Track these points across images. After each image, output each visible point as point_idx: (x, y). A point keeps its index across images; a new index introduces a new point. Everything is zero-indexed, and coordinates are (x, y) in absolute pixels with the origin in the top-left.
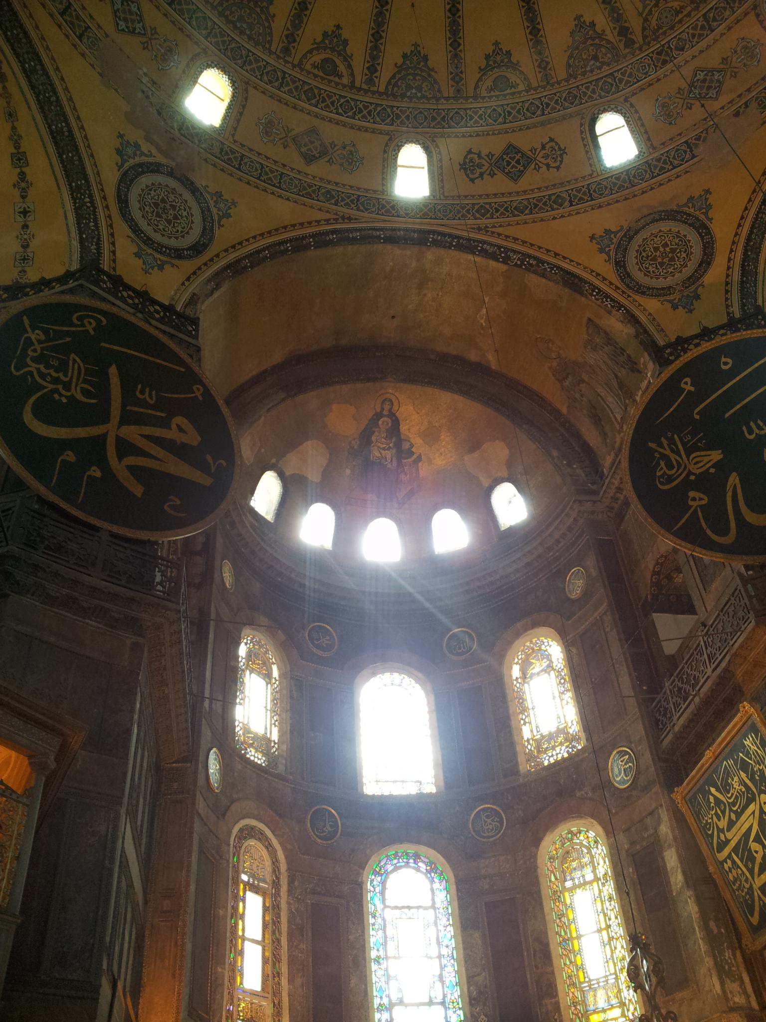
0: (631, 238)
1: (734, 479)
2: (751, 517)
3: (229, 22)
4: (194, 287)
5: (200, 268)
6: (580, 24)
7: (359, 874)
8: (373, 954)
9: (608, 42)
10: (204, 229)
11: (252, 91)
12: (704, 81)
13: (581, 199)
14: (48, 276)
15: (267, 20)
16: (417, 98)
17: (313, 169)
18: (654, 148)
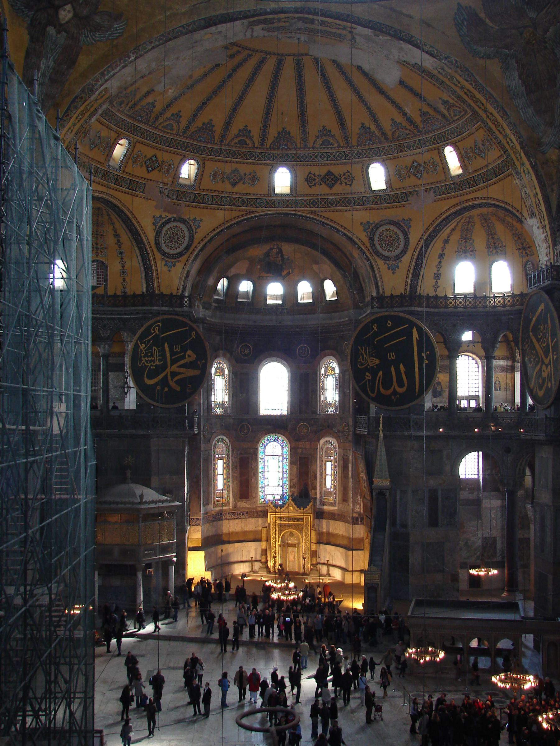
0: (378, 228)
1: (380, 373)
2: (382, 390)
3: (194, 140)
4: (187, 268)
5: (189, 257)
6: (363, 126)
7: (257, 445)
8: (260, 471)
9: (376, 136)
10: (190, 237)
11: (206, 162)
12: (416, 167)
13: (359, 203)
14: (137, 293)
15: (212, 133)
16: (286, 149)
17: (237, 189)
18: (392, 190)
